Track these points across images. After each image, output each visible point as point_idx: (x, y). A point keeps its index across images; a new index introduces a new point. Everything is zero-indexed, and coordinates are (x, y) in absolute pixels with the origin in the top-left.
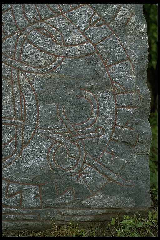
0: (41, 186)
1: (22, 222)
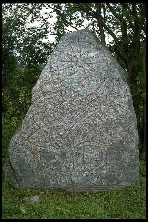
0: (107, 179)
1: (101, 190)
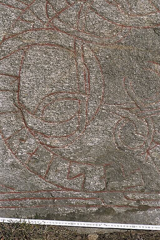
0: (106, 166)
